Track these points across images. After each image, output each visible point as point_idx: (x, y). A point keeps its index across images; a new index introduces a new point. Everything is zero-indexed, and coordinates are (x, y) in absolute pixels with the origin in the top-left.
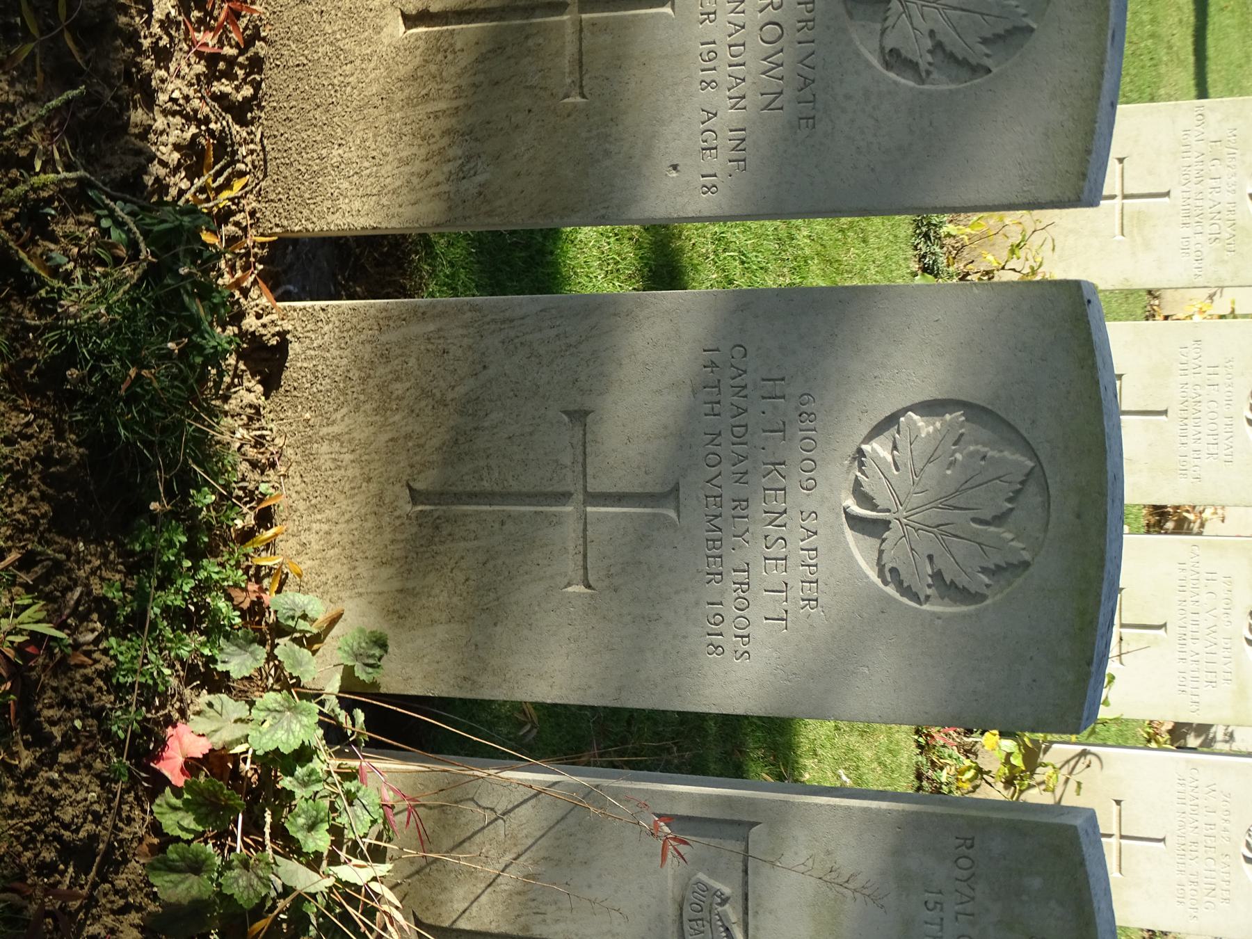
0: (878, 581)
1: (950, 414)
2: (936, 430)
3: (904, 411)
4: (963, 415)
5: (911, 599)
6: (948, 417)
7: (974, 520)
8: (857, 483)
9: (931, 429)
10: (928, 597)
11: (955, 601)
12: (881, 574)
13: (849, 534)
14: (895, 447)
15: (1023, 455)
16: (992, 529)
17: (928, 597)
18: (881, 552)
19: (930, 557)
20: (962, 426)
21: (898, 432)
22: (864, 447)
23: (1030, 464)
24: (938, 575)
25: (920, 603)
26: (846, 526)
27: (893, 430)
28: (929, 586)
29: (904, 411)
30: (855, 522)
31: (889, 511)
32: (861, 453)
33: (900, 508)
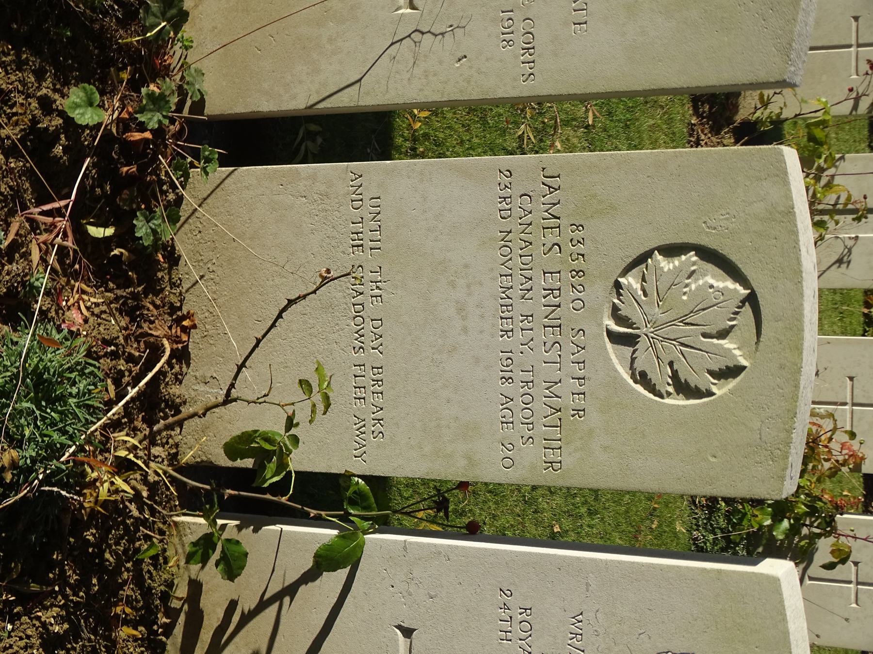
0: (631, 382)
1: (685, 255)
2: (675, 267)
3: (649, 254)
4: (696, 255)
5: (655, 395)
6: (683, 257)
7: (705, 335)
8: (615, 309)
9: (671, 266)
10: (669, 394)
11: (688, 397)
12: (633, 376)
13: (609, 345)
14: (644, 279)
15: (740, 285)
16: (715, 341)
17: (669, 394)
18: (633, 360)
19: (671, 364)
20: (694, 264)
21: (647, 270)
22: (622, 280)
23: (748, 291)
24: (675, 376)
25: (662, 397)
26: (607, 340)
27: (644, 266)
28: (669, 384)
29: (649, 254)
30: (614, 337)
31: (638, 328)
32: (618, 286)
33: (649, 326)
